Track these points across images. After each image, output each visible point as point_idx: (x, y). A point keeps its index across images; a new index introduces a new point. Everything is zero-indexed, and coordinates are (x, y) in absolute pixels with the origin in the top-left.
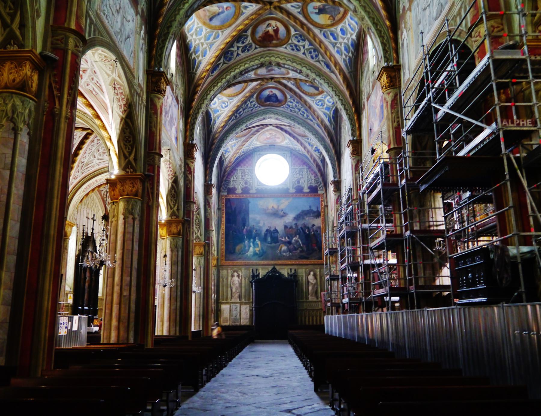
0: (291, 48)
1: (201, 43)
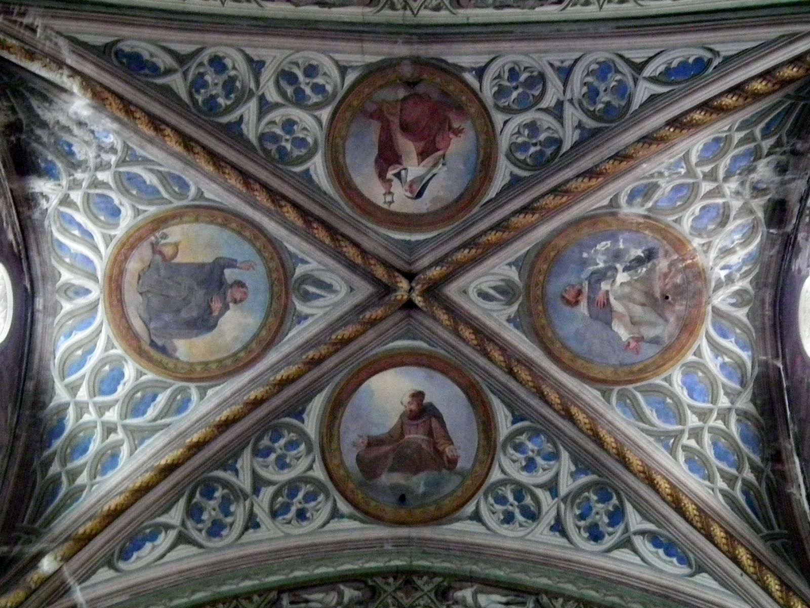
0: (320, 80)
1: (715, 180)
